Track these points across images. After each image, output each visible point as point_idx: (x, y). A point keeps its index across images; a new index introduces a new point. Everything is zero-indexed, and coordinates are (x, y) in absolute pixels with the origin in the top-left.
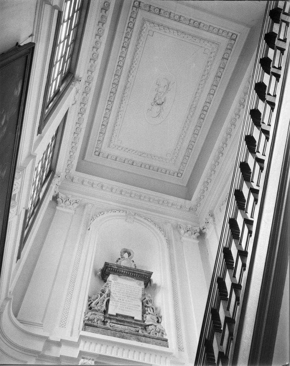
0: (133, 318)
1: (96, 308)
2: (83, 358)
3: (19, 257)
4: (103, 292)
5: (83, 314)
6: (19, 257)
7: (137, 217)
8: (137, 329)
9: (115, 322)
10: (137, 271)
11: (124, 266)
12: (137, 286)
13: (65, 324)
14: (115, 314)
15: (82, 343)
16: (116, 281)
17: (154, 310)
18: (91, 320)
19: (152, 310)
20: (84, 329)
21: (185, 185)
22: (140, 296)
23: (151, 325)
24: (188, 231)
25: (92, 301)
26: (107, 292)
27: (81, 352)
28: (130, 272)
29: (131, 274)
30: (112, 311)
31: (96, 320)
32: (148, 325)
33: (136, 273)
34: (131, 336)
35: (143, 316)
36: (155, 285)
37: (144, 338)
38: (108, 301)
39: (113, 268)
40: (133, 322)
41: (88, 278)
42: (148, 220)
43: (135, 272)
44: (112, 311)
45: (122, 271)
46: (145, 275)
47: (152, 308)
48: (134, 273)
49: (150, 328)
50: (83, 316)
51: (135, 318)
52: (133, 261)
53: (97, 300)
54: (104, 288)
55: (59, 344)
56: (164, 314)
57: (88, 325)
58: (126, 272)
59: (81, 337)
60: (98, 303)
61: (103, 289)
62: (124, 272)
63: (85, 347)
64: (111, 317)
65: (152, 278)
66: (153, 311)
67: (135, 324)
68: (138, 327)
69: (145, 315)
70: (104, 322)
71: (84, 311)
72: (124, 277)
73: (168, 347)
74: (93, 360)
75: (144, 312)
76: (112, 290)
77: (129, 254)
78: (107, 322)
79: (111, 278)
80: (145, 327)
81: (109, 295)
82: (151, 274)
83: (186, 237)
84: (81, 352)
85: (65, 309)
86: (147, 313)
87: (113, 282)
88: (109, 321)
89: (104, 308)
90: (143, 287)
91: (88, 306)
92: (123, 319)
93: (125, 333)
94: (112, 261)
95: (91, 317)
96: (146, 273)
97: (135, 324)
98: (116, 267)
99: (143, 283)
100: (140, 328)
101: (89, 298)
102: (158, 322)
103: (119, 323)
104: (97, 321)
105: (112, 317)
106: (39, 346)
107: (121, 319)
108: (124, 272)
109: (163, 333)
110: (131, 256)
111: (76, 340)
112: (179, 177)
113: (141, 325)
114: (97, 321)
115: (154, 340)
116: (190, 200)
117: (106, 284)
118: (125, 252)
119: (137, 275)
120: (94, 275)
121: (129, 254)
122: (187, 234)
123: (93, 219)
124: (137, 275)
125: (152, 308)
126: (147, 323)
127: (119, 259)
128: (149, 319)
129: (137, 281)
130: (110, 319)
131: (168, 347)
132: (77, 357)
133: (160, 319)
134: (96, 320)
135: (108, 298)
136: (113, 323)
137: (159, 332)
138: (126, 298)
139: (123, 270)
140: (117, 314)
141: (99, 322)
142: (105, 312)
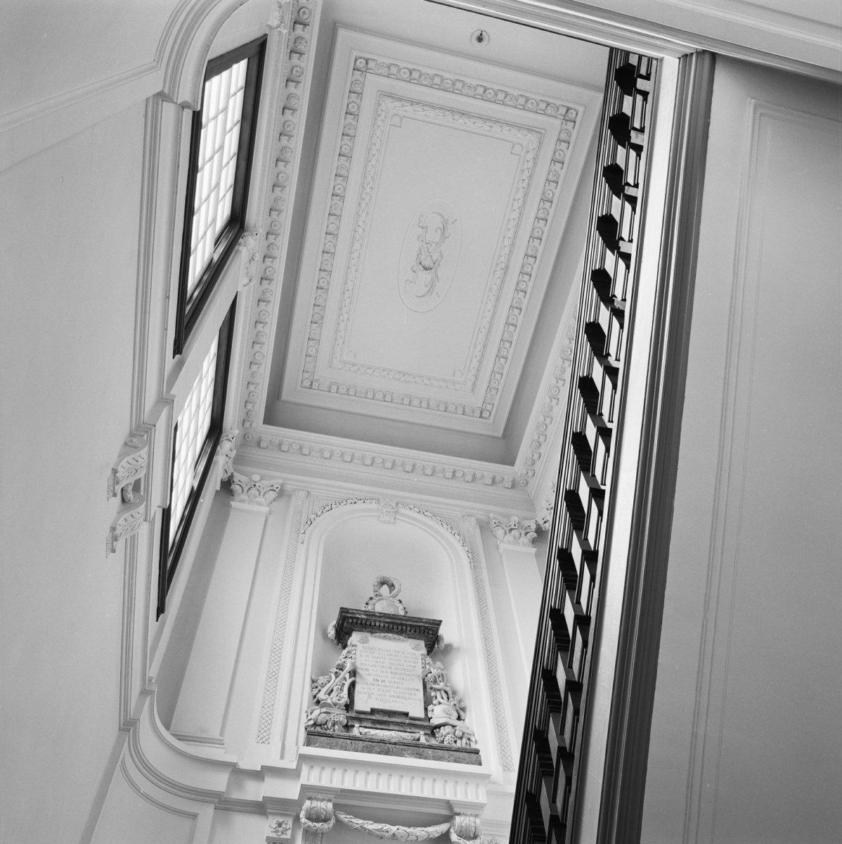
0: (406, 714)
1: (329, 701)
2: (310, 799)
3: (161, 609)
4: (341, 668)
5: (304, 715)
6: (161, 609)
7: (402, 510)
8: (417, 736)
9: (370, 725)
10: (408, 621)
11: (380, 613)
12: (410, 650)
13: (267, 737)
14: (369, 710)
15: (305, 769)
17: (450, 695)
18: (320, 725)
19: (445, 696)
20: (308, 743)
21: (500, 434)
22: (419, 671)
23: (444, 725)
24: (511, 530)
25: (319, 688)
26: (348, 667)
27: (304, 788)
28: (393, 623)
29: (395, 627)
30: (362, 704)
31: (330, 725)
32: (439, 727)
33: (406, 625)
34: (405, 750)
35: (426, 709)
36: (449, 648)
37: (430, 751)
38: (353, 685)
39: (358, 618)
40: (407, 721)
42: (426, 514)
43: (404, 622)
44: (362, 704)
45: (377, 624)
46: (426, 628)
47: (446, 692)
48: (402, 625)
49: (443, 731)
50: (304, 719)
51: (410, 715)
52: (400, 602)
53: (329, 685)
54: (343, 660)
55: (259, 775)
56: (470, 704)
57: (316, 733)
58: (387, 625)
59: (303, 758)
60: (332, 691)
61: (339, 662)
62: (382, 625)
63: (312, 777)
64: (361, 717)
65: (441, 632)
66: (448, 698)
67: (410, 725)
68: (417, 731)
69: (430, 708)
70: (348, 727)
71: (305, 708)
72: (383, 634)
73: (480, 764)
74: (329, 800)
75: (428, 701)
77: (392, 586)
78: (353, 726)
79: (355, 638)
80: (433, 730)
81: (353, 673)
82: (439, 623)
83: (509, 543)
84: (304, 788)
85: (266, 707)
86: (435, 702)
87: (360, 646)
88: (357, 725)
90: (424, 651)
91: (312, 698)
92: (386, 718)
93: (390, 743)
94: (357, 604)
95: (322, 719)
96: (426, 623)
98: (364, 617)
99: (422, 643)
100: (422, 732)
101: (313, 681)
102: (459, 718)
103: (378, 726)
104: (334, 725)
105: (363, 716)
106: (218, 782)
108: (382, 625)
109: (469, 739)
110: (396, 590)
111: (293, 766)
112: (486, 418)
114: (334, 725)
115: (451, 753)
116: (512, 463)
117: (345, 652)
118: (383, 583)
119: (409, 628)
120: (320, 637)
121: (392, 586)
122: (509, 537)
123: (309, 522)
124: (409, 628)
125: (446, 692)
126: (435, 722)
127: (371, 598)
128: (439, 714)
129: (410, 641)
130: (360, 720)
131: (480, 764)
132: (297, 799)
133: (462, 713)
134: (330, 725)
136: (365, 727)
137: (461, 738)
139: (380, 621)
140: (373, 711)
141: (336, 727)
142: (349, 707)
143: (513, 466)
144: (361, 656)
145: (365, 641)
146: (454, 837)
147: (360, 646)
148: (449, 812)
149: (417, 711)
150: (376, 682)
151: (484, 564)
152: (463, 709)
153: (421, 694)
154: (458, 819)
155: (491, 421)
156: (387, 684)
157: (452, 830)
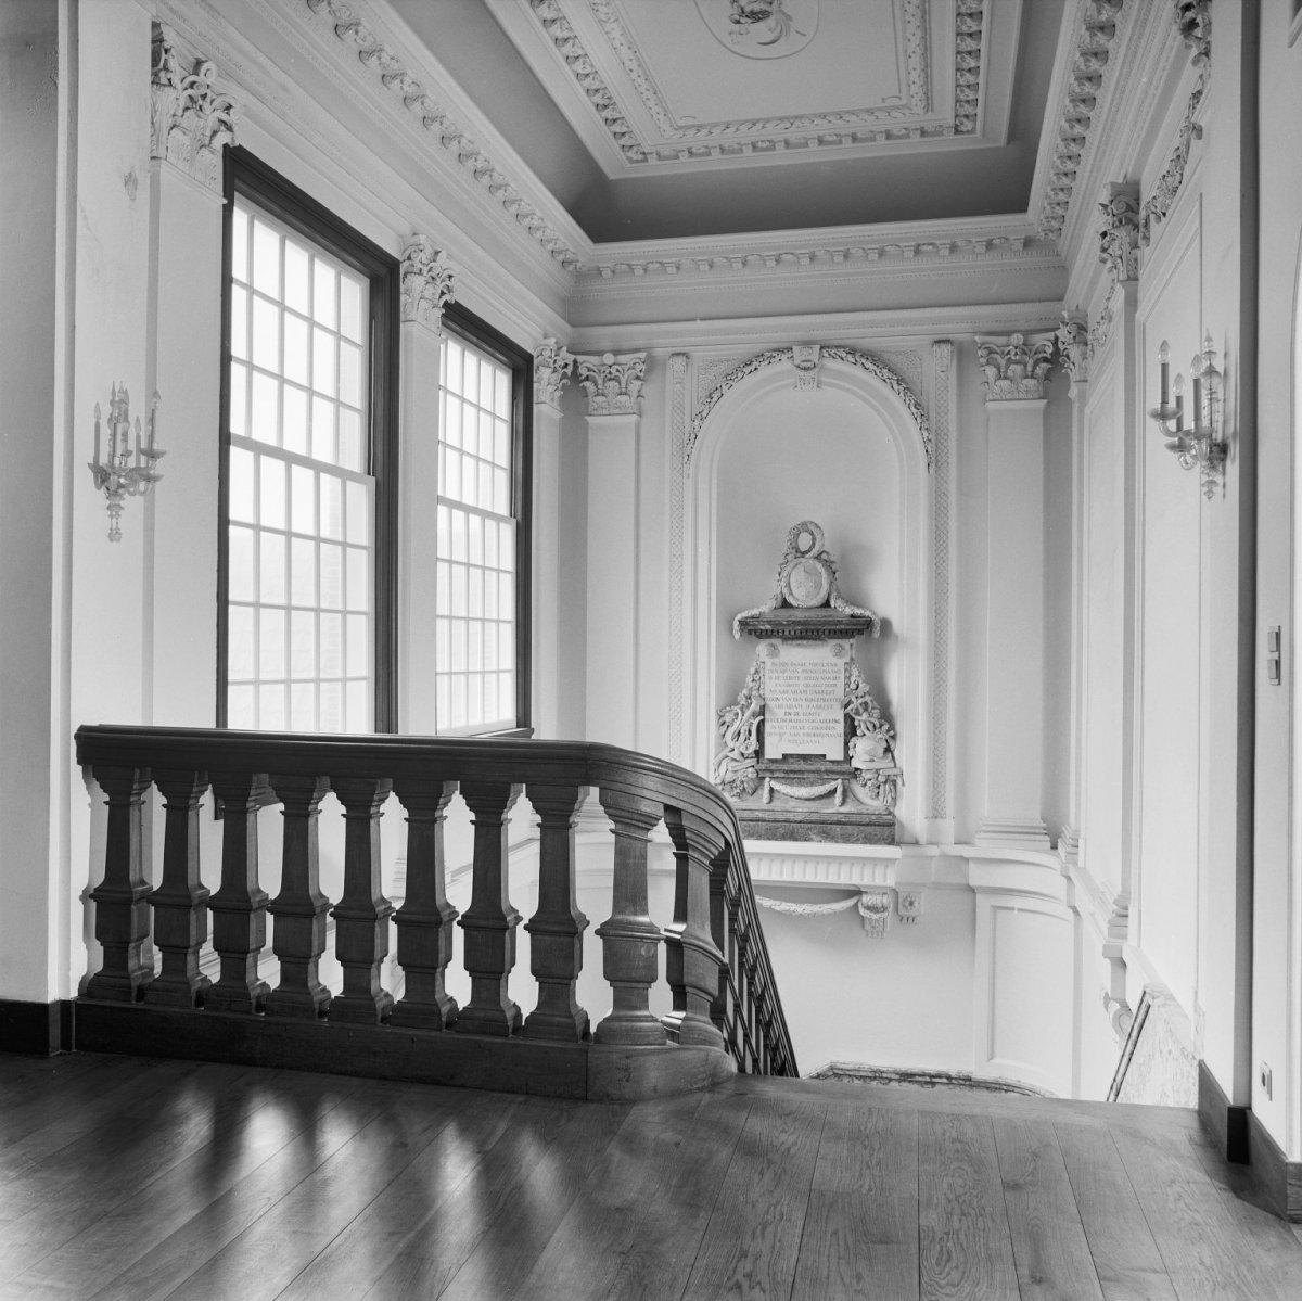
0: (824, 756)
9: (783, 775)
16: (776, 660)
22: (840, 692)
30: (773, 751)
31: (738, 783)
35: (846, 744)
37: (838, 828)
38: (762, 722)
40: (823, 768)
41: (709, 673)
44: (773, 751)
51: (827, 758)
60: (739, 734)
71: (712, 760)
75: (851, 731)
76: (768, 695)
78: (764, 778)
81: (762, 711)
86: (859, 732)
89: (753, 744)
97: (827, 772)
98: (768, 627)
107: (797, 767)
112: (968, 132)
113: (843, 773)
115: (862, 828)
123: (693, 436)
130: (772, 771)
135: (762, 717)
138: (804, 704)
142: (759, 753)
143: (1025, 210)
144: (771, 678)
145: (774, 652)
146: (862, 911)
147: (769, 661)
148: (855, 892)
149: (835, 753)
150: (788, 717)
151: (953, 460)
152: (893, 737)
153: (840, 728)
154: (865, 899)
155: (978, 134)
156: (801, 717)
157: (860, 905)
